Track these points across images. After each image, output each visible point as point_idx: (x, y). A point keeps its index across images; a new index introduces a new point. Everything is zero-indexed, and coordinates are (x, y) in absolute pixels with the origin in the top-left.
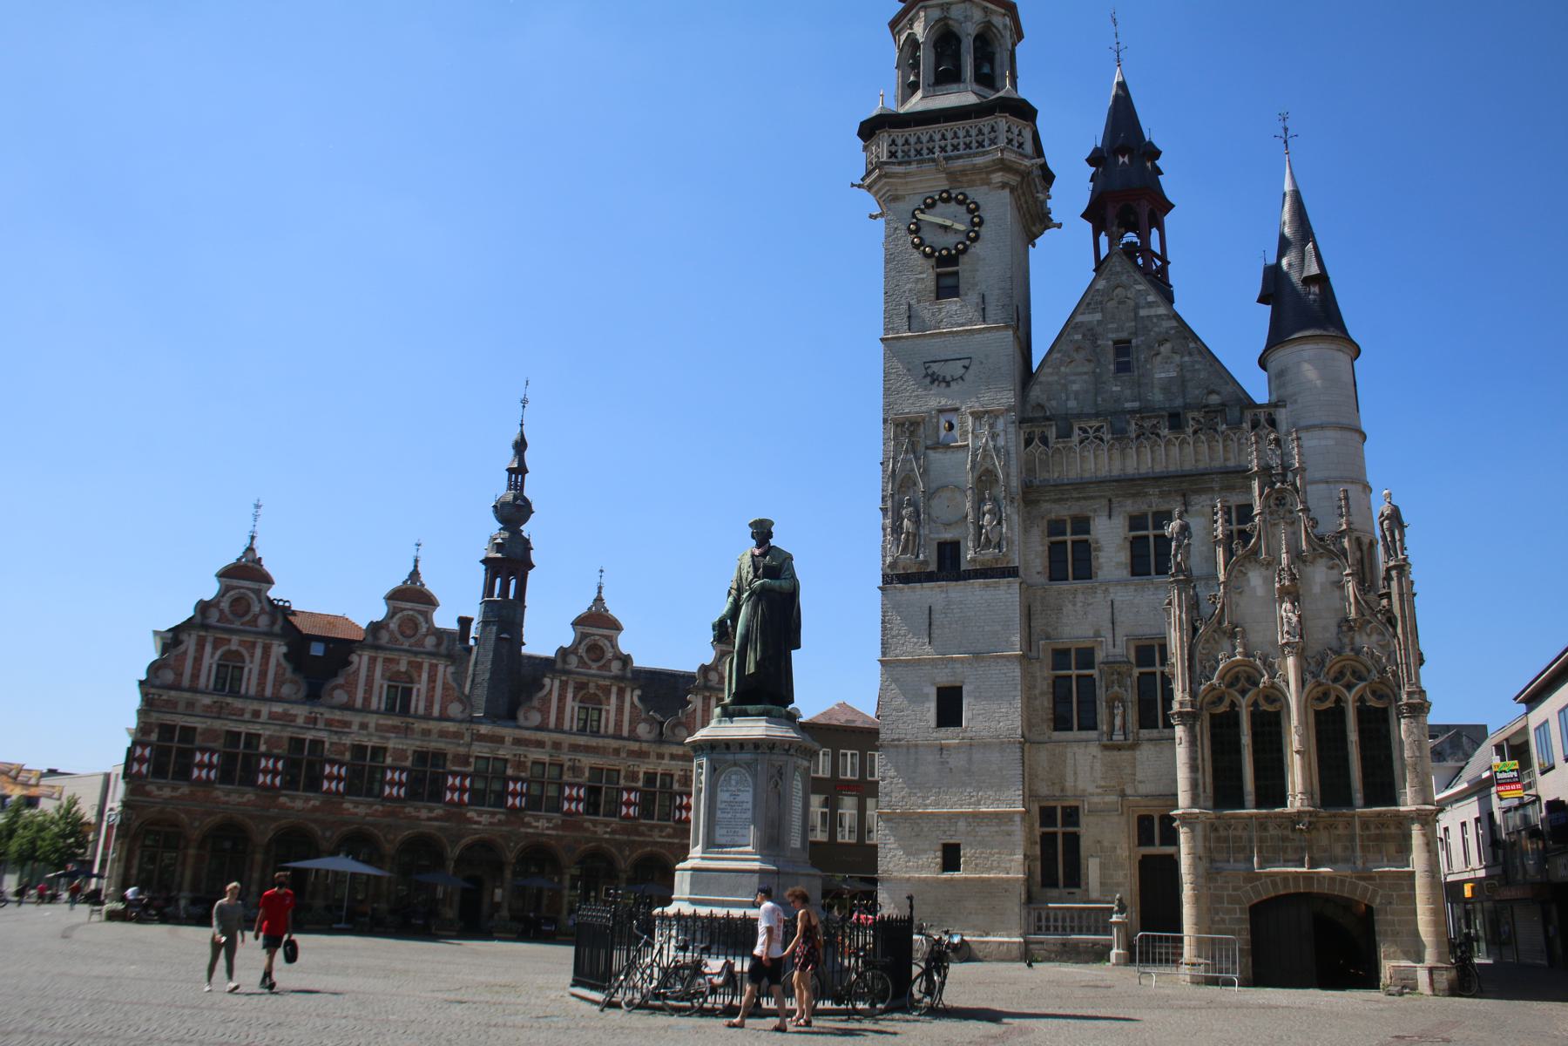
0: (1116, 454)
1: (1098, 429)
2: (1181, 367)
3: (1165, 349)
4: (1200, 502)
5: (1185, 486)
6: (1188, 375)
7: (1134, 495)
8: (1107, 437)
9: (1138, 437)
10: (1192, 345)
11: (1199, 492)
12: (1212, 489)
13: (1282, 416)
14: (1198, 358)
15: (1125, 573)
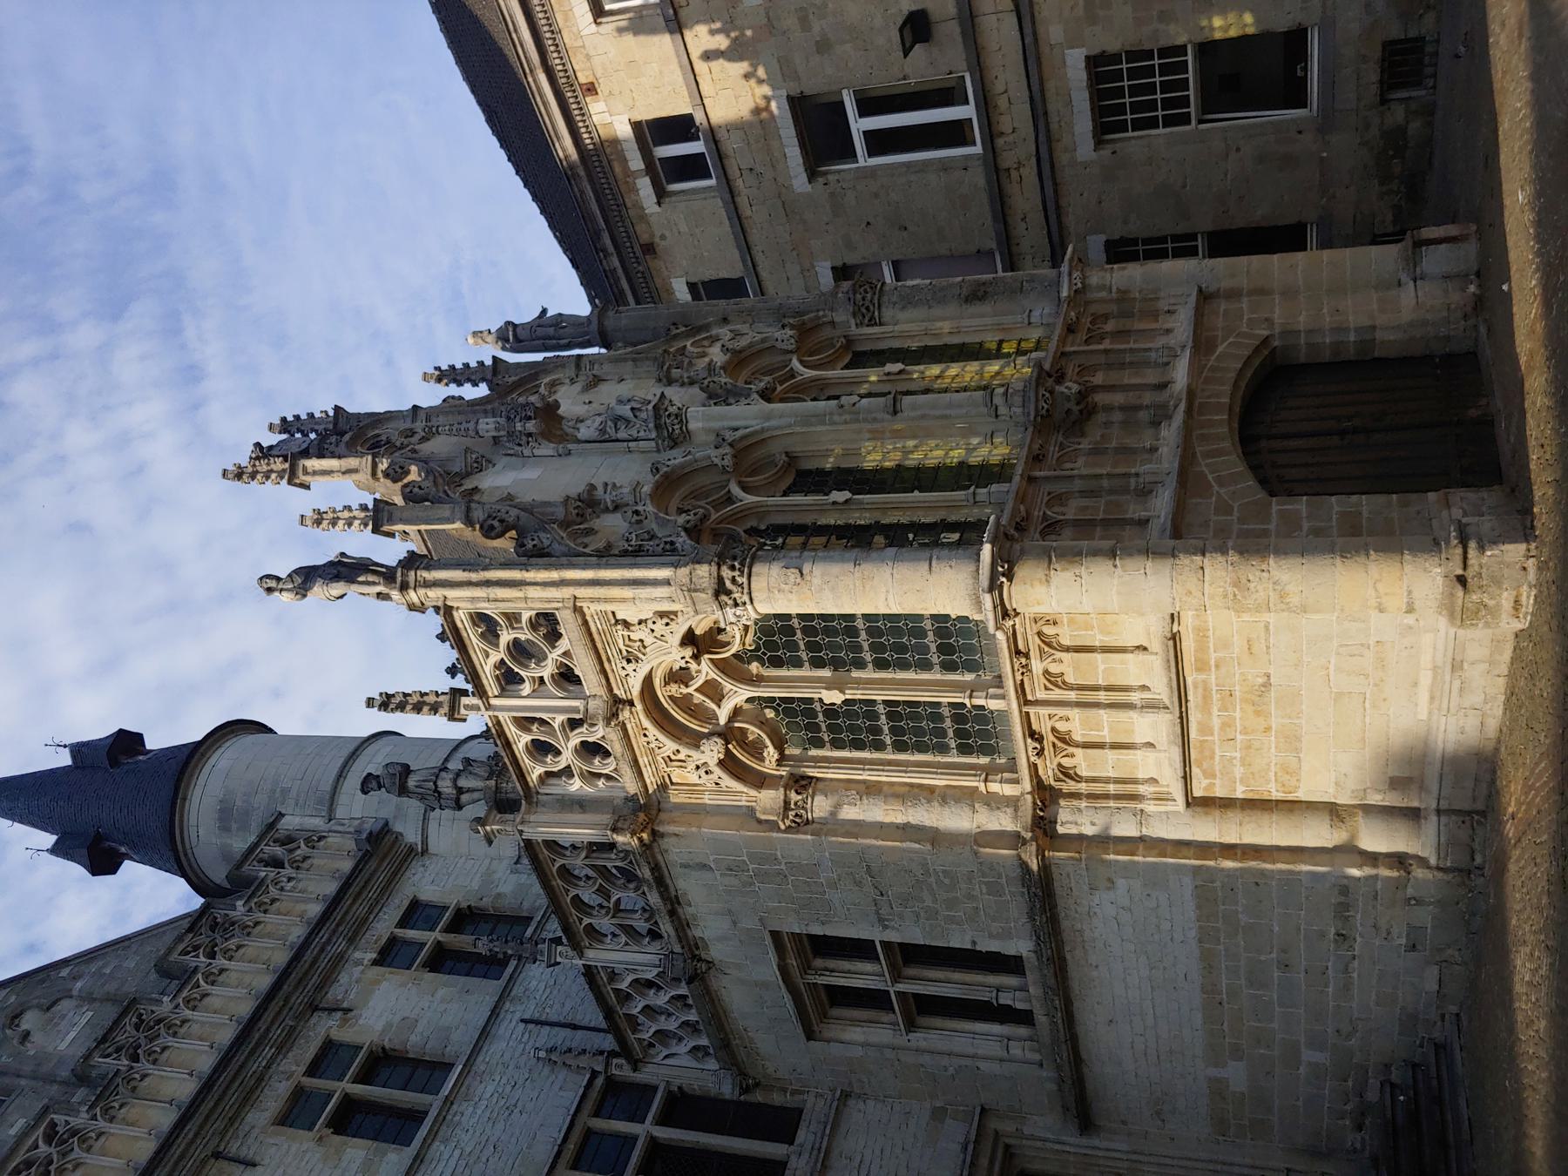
0: (135, 1110)
1: (49, 1138)
2: (88, 998)
3: (29, 1021)
4: (346, 985)
5: (298, 1000)
6: (111, 987)
7: (248, 1099)
8: (80, 1120)
9: (135, 1058)
10: (64, 973)
11: (328, 980)
12: (339, 960)
13: (290, 823)
14: (93, 968)
15: (395, 1159)
